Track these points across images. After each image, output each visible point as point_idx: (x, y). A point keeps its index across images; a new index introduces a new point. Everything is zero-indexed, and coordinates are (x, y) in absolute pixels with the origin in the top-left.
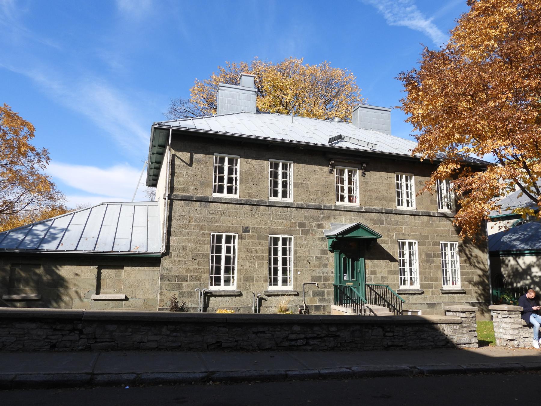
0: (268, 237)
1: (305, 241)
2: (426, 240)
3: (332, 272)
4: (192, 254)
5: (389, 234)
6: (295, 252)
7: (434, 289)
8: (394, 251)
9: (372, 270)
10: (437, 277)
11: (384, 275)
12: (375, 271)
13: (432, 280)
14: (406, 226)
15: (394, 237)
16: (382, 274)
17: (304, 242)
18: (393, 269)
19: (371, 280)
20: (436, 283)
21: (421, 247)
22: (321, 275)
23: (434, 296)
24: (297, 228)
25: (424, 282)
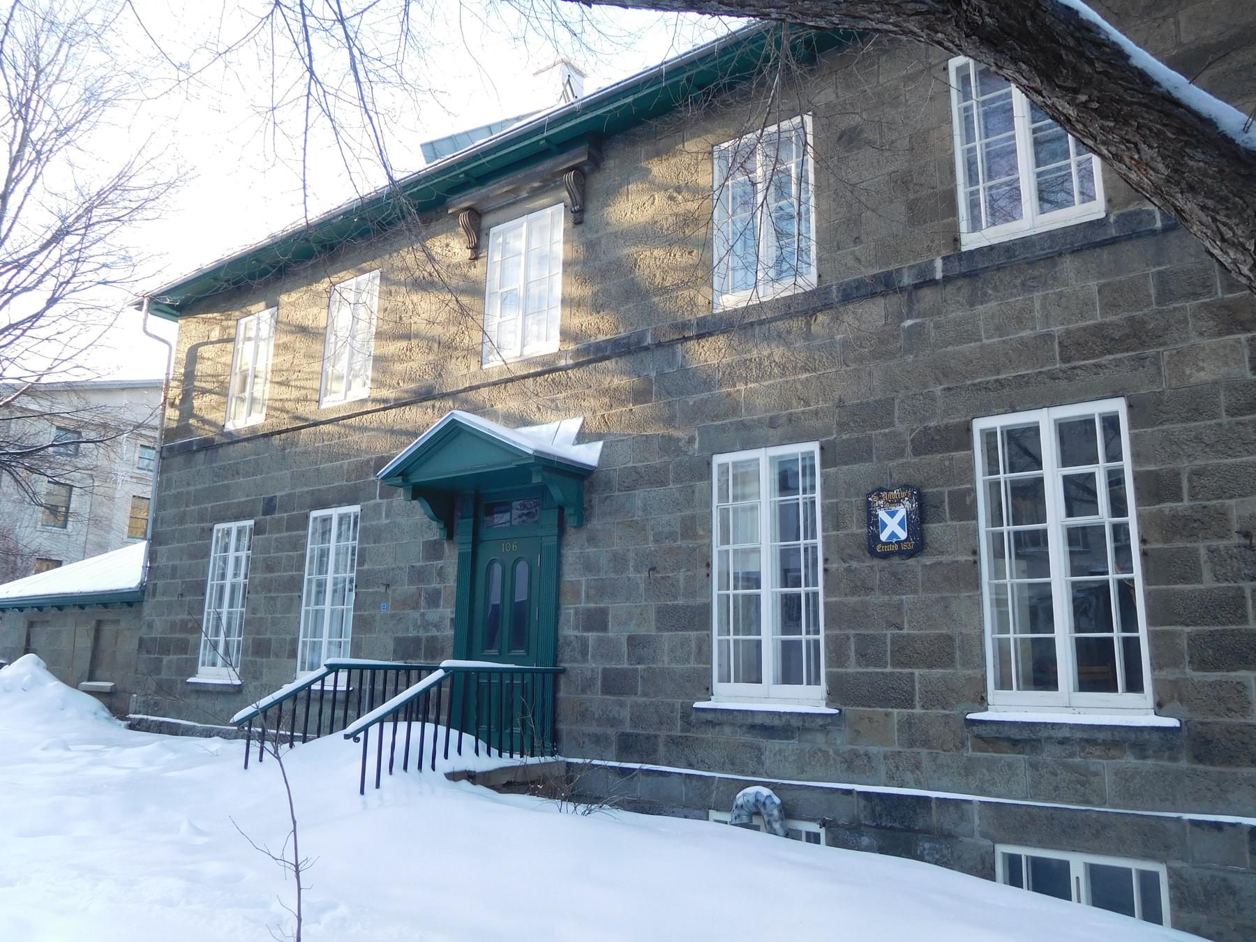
1: (387, 516)
4: (183, 582)
7: (918, 710)
8: (689, 512)
9: (588, 610)
10: (950, 638)
11: (642, 631)
12: (603, 612)
13: (905, 653)
15: (696, 446)
16: (633, 629)
17: (384, 521)
18: (681, 601)
19: (584, 653)
21: (842, 472)
22: (422, 634)
23: (924, 752)
25: (852, 669)
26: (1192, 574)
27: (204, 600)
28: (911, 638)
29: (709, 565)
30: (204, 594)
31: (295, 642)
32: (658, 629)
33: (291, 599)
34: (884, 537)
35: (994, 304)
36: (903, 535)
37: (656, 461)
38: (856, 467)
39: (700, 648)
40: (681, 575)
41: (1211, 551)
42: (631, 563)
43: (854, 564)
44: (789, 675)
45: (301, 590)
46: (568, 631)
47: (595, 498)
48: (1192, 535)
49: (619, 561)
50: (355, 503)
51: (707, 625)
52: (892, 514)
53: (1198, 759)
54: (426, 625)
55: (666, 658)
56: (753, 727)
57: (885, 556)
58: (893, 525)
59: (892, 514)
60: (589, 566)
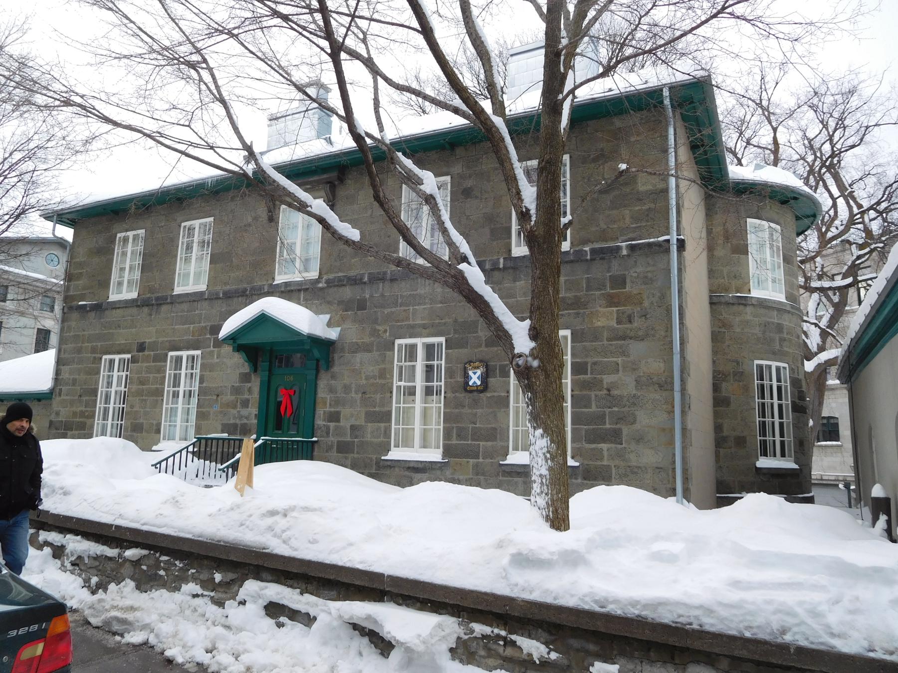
0: (167, 355)
2: (469, 333)
3: (256, 415)
4: (81, 389)
5: (375, 329)
6: (201, 381)
7: (481, 460)
8: (383, 366)
9: (331, 412)
10: (495, 429)
11: (357, 423)
13: (477, 435)
14: (419, 304)
15: (388, 334)
16: (353, 422)
17: (216, 360)
18: (377, 409)
19: (328, 433)
20: (489, 444)
21: (454, 352)
22: (238, 422)
23: (482, 478)
24: (208, 336)
25: (454, 442)
26: (588, 406)
27: (96, 400)
28: (480, 428)
29: (391, 392)
30: (96, 396)
31: (159, 425)
32: (366, 422)
33: (157, 401)
34: (471, 383)
35: (522, 282)
36: (479, 383)
37: (367, 340)
38: (460, 350)
39: (385, 432)
40: (378, 396)
41: (596, 396)
42: (353, 390)
43: (457, 394)
44: (425, 445)
45: (163, 396)
46: (320, 422)
47: (336, 356)
48: (590, 389)
49: (347, 389)
50: (197, 349)
51: (390, 420)
52: (475, 373)
53: (585, 479)
54: (241, 417)
55: (369, 436)
56: (409, 468)
57: (471, 392)
58: (475, 378)
59: (475, 373)
60: (331, 390)
